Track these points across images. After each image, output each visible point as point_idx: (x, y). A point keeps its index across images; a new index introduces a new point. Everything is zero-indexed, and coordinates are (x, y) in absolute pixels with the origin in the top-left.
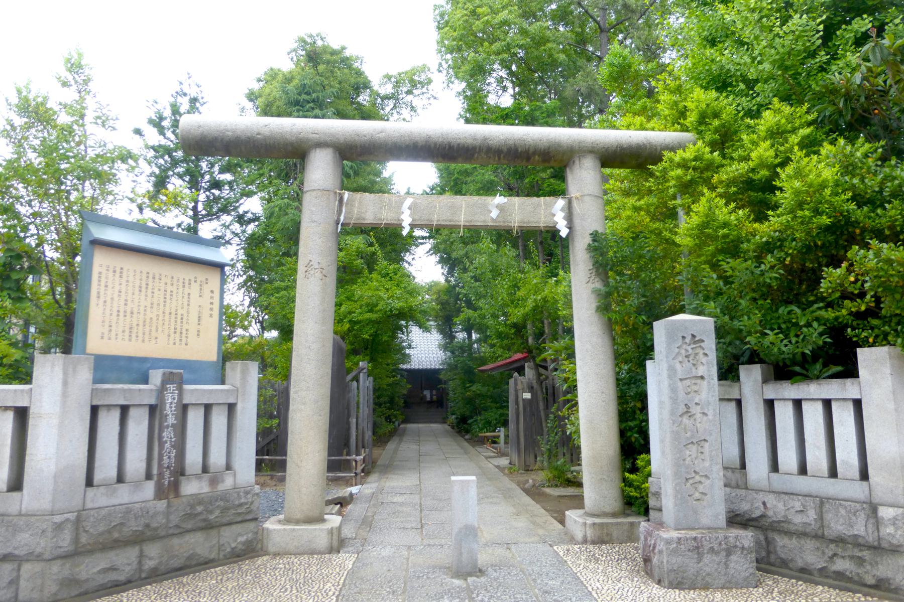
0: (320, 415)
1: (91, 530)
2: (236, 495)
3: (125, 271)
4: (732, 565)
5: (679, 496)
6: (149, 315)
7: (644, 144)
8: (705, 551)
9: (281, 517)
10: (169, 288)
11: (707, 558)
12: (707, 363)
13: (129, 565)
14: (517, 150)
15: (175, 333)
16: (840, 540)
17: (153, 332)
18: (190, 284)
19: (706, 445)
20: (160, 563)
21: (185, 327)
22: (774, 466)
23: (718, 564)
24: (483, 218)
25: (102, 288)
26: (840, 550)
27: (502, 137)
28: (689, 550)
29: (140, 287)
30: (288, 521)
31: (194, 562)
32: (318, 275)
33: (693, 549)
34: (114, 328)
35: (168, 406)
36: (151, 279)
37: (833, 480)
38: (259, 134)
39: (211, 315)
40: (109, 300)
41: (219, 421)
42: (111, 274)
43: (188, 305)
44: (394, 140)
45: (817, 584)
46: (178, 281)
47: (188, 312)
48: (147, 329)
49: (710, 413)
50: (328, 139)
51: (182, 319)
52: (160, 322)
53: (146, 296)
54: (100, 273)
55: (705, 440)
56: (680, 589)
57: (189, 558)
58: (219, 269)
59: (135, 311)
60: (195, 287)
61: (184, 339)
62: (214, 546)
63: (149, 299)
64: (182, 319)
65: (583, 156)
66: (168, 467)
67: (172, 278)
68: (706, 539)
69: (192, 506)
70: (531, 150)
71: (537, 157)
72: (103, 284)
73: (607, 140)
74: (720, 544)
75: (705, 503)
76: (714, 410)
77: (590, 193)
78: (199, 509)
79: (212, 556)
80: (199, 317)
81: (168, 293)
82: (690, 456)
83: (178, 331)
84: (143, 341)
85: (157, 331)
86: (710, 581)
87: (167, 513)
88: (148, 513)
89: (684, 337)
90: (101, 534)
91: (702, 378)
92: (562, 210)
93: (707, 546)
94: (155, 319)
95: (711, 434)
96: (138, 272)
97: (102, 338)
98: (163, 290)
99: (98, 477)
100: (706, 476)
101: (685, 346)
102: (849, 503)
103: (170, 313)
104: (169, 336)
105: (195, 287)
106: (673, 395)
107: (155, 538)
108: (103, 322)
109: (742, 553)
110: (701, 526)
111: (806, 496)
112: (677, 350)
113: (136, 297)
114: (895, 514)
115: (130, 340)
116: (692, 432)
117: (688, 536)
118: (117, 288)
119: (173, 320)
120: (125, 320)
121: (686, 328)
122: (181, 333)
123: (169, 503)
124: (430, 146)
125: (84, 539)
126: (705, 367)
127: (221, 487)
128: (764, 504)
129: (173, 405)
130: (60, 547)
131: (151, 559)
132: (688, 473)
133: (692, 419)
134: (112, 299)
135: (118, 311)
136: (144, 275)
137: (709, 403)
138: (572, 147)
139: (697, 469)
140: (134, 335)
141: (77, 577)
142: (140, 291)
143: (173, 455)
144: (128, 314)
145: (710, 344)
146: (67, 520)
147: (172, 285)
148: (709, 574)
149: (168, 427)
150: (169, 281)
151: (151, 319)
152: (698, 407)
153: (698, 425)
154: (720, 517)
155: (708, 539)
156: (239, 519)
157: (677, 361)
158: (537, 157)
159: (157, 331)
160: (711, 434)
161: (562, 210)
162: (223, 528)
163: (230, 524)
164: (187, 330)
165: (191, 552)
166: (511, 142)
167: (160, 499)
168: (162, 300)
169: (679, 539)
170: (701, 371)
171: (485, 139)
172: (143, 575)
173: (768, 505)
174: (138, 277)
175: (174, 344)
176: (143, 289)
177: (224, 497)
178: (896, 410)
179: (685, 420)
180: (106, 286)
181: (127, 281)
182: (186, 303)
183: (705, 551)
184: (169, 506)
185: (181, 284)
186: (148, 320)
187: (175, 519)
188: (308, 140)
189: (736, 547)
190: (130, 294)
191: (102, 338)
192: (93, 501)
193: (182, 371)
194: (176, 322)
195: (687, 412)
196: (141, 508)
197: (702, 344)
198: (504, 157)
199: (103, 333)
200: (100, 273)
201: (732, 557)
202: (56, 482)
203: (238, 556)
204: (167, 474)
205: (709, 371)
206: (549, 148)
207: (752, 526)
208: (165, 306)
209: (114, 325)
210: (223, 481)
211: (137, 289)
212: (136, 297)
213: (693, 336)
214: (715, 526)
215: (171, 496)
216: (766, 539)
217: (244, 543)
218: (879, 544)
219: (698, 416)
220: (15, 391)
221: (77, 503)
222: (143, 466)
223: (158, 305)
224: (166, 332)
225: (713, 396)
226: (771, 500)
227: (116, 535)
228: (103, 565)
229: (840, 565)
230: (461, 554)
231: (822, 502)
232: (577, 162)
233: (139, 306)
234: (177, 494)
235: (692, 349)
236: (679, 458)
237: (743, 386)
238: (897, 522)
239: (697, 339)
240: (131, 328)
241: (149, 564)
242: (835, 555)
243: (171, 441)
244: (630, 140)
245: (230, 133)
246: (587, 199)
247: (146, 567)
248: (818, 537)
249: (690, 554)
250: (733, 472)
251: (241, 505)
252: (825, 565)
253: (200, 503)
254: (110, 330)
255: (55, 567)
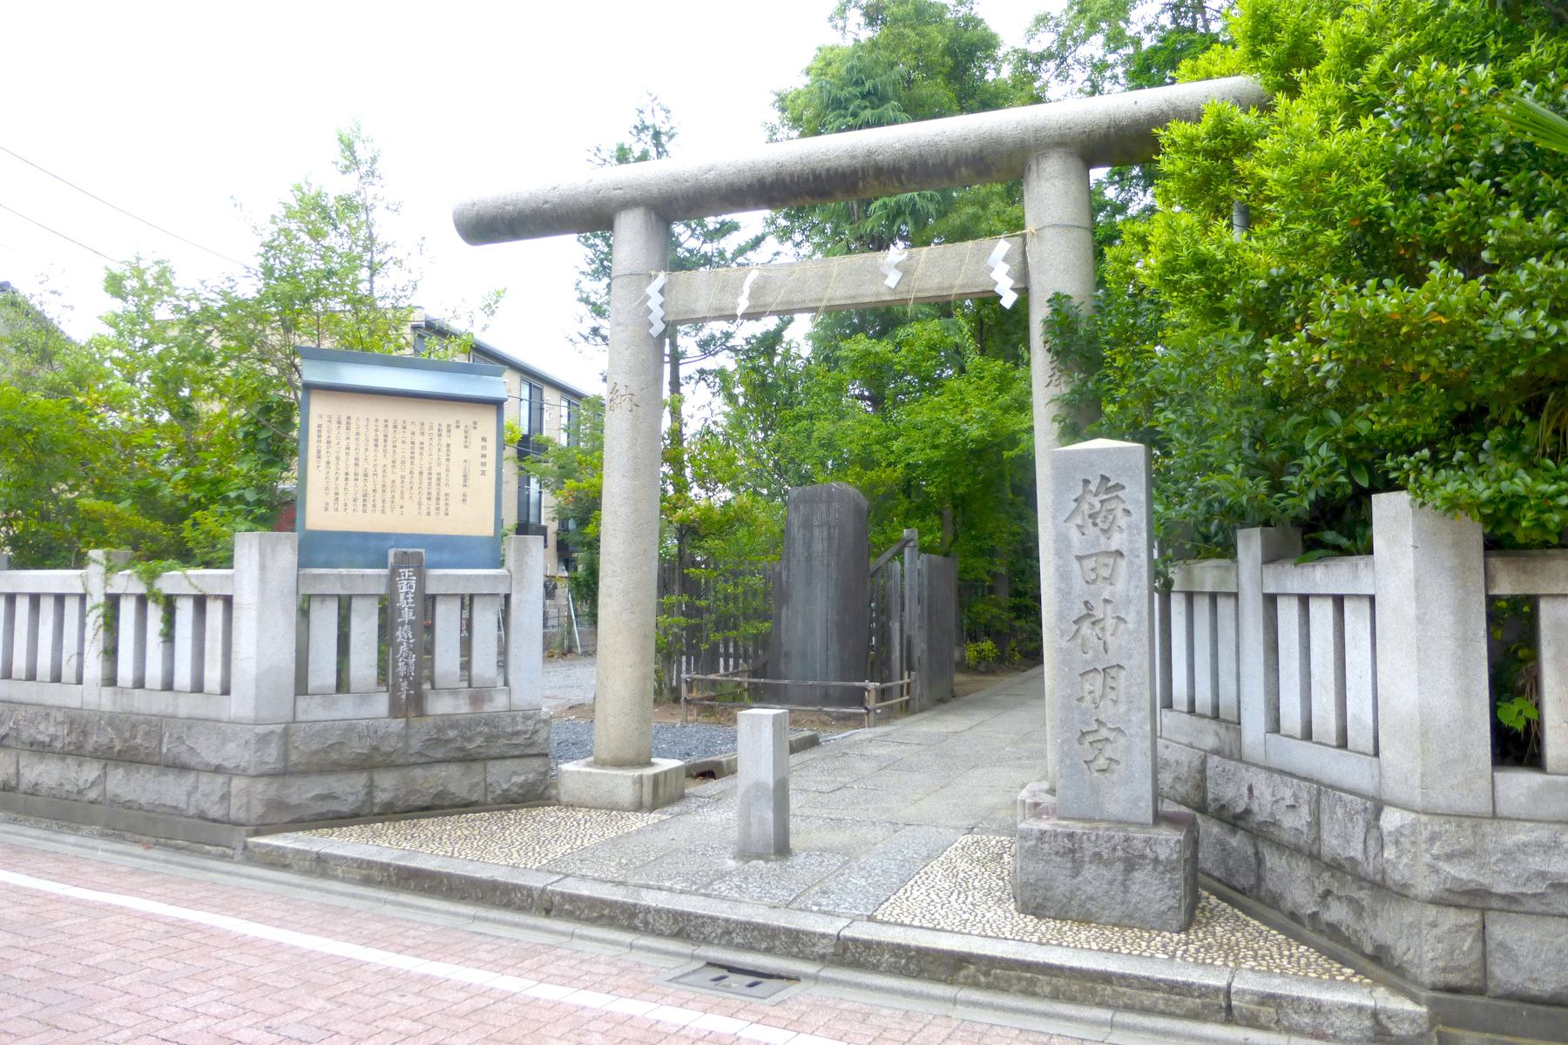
0: (633, 613)
1: (301, 747)
2: (509, 720)
3: (353, 421)
4: (1135, 888)
5: (1068, 762)
6: (390, 476)
7: (1162, 112)
8: (1087, 859)
9: (591, 759)
10: (418, 439)
11: (1089, 871)
12: (1130, 527)
13: (353, 794)
14: (925, 163)
15: (429, 499)
16: (1336, 867)
17: (397, 500)
18: (449, 431)
19: (1123, 674)
20: (396, 797)
21: (444, 490)
22: (1275, 726)
23: (1111, 883)
24: (874, 289)
25: (324, 445)
26: (1336, 885)
27: (898, 146)
28: (1057, 853)
29: (376, 440)
30: (595, 763)
31: (447, 803)
32: (626, 405)
33: (1065, 853)
34: (341, 496)
35: (402, 597)
36: (390, 429)
37: (56, 685)
38: (546, 202)
39: (483, 473)
40: (333, 459)
41: (485, 620)
42: (334, 426)
43: (448, 460)
44: (729, 179)
45: (1302, 941)
46: (431, 428)
47: (447, 470)
48: (388, 496)
49: (1131, 617)
50: (636, 194)
51: (439, 479)
52: (407, 485)
53: (385, 451)
54: (320, 426)
55: (1119, 666)
56: (1040, 917)
57: (438, 795)
58: (494, 407)
59: (370, 472)
60: (458, 435)
61: (442, 507)
62: (478, 784)
63: (389, 456)
64: (439, 479)
65: (1043, 155)
66: (405, 677)
67: (423, 424)
68: (1089, 839)
69: (441, 729)
70: (951, 160)
71: (963, 169)
72: (324, 439)
73: (1089, 117)
74: (1114, 849)
75: (1115, 777)
76: (1138, 613)
77: (1055, 221)
78: (452, 734)
79: (474, 798)
80: (465, 476)
81: (417, 446)
82: (1091, 692)
83: (434, 497)
84: (383, 512)
85: (402, 498)
86: (1094, 910)
87: (405, 736)
88: (376, 732)
89: (1086, 482)
90: (316, 753)
91: (1119, 554)
92: (1006, 259)
93: (1089, 849)
94: (398, 481)
95: (1131, 657)
96: (372, 420)
97: (326, 509)
98: (408, 441)
99: (314, 682)
100: (1119, 730)
101: (1090, 498)
102: (1351, 797)
103: (421, 473)
104: (420, 503)
105: (458, 435)
106: (1063, 586)
107: (389, 765)
108: (327, 488)
109: (1155, 869)
110: (1106, 816)
111: (1305, 779)
112: (1074, 505)
113: (371, 453)
114: (1399, 824)
115: (364, 511)
116: (1095, 650)
117: (1059, 830)
118: (344, 444)
119: (425, 482)
120: (356, 485)
121: (1091, 465)
122: (438, 499)
123: (407, 724)
124: (783, 180)
125: (294, 757)
126: (1125, 535)
127: (488, 708)
128: (1250, 789)
129: (410, 596)
130: (267, 763)
131: (384, 790)
132: (1085, 723)
133: (1097, 628)
134: (338, 458)
135: (347, 474)
136: (381, 425)
137: (1129, 601)
138: (1022, 141)
139: (1102, 717)
140: (369, 505)
141: (287, 800)
142: (376, 446)
143: (412, 661)
144: (361, 477)
145: (1136, 492)
146: (272, 732)
147: (423, 434)
148: (1091, 898)
149: (403, 624)
150: (417, 430)
151: (393, 481)
152: (1109, 607)
153: (1109, 639)
154: (1142, 804)
155: (1093, 838)
156: (517, 753)
157: (1072, 525)
158: (963, 169)
159: (402, 498)
160: (1131, 657)
161: (1006, 259)
162: (490, 764)
163: (503, 758)
164: (446, 495)
165: (441, 788)
166: (914, 152)
167: (396, 718)
168: (408, 455)
169: (1043, 833)
170: (1117, 541)
171: (870, 154)
172: (376, 810)
173: (1256, 792)
174: (372, 427)
175: (429, 514)
176: (381, 443)
177: (491, 721)
178: (1419, 619)
179: (1086, 628)
180: (329, 442)
181: (358, 434)
182: (444, 458)
183: (1087, 859)
184: (408, 725)
185: (435, 431)
186: (389, 484)
187: (416, 744)
188: (610, 200)
189: (1143, 857)
190: (362, 450)
191: (326, 509)
192: (305, 712)
193: (423, 551)
194: (429, 484)
195: (1089, 616)
196: (367, 727)
197: (1120, 493)
198: (907, 178)
199: (327, 504)
200: (320, 426)
201: (1136, 874)
202: (258, 687)
203: (513, 802)
204: (404, 686)
205: (1131, 542)
206: (981, 151)
207: (1242, 829)
208: (412, 463)
209: (341, 491)
210: (491, 700)
211: (371, 443)
212: (371, 453)
213: (1104, 478)
214: (1132, 818)
215: (412, 714)
216: (1257, 853)
217: (521, 786)
218: (1383, 879)
219: (1110, 623)
220: (221, 576)
221: (285, 713)
222: (373, 673)
223: (403, 462)
224: (416, 498)
225: (1137, 587)
226: (1260, 781)
227: (334, 756)
228: (318, 791)
229: (1337, 913)
230: (749, 824)
231: (1322, 789)
232: (1034, 167)
233: (375, 465)
234: (421, 713)
235: (1102, 502)
236: (1069, 696)
237: (1241, 567)
238: (1402, 840)
239: (1110, 484)
240: (365, 495)
241: (382, 797)
242: (1328, 893)
243: (408, 643)
244: (1136, 108)
245: (510, 208)
246: (1048, 233)
247: (378, 800)
248: (1314, 857)
249: (1059, 859)
250: (1227, 728)
251: (517, 733)
252: (1315, 909)
253: (452, 727)
254: (337, 499)
255: (260, 785)
